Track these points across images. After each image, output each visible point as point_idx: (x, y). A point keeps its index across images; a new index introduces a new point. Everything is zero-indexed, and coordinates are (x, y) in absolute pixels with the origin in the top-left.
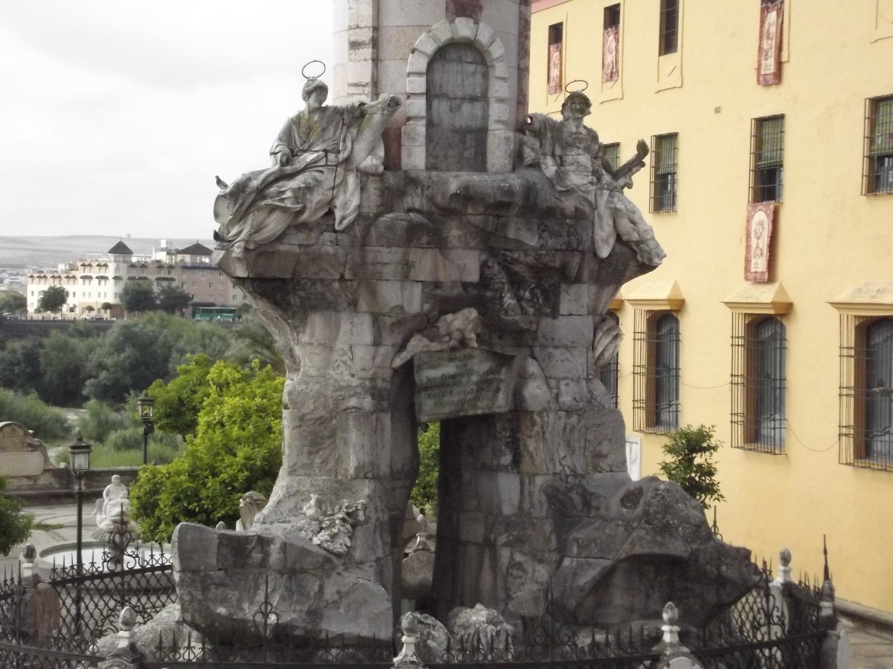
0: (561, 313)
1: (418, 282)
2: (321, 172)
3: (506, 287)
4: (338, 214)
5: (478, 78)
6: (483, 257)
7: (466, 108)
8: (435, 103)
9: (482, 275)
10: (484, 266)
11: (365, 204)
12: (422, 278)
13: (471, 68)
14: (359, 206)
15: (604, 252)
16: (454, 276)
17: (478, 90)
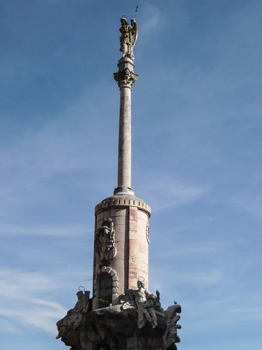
0: (128, 347)
1: (91, 341)
2: (74, 315)
3: (112, 341)
4: (75, 325)
5: (110, 282)
6: (105, 332)
7: (107, 290)
8: (101, 291)
9: (105, 338)
10: (105, 335)
11: (82, 321)
12: (93, 340)
13: (108, 280)
14: (81, 322)
15: (140, 326)
16: (98, 338)
17: (110, 285)
